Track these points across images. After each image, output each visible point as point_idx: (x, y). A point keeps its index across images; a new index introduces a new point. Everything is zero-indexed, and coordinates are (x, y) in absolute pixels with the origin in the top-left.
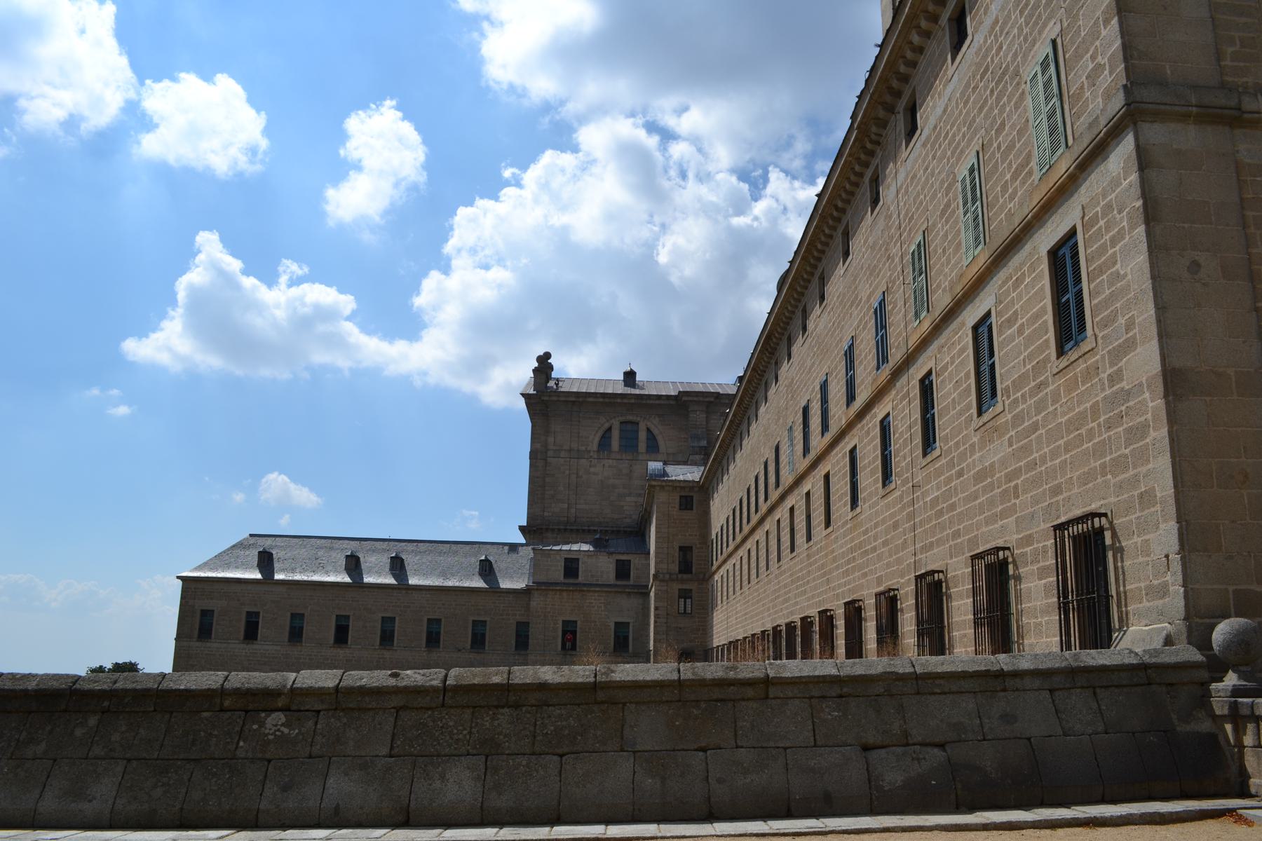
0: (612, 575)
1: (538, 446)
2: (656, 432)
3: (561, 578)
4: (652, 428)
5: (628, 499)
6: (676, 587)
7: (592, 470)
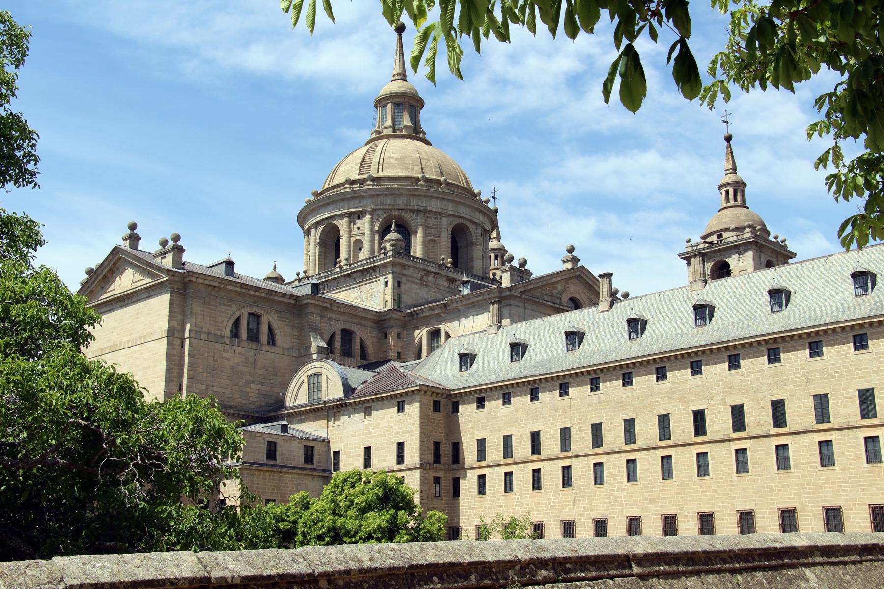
0: (302, 459)
1: (175, 324)
2: (275, 326)
3: (265, 461)
4: (272, 322)
5: (253, 386)
6: (433, 474)
7: (225, 355)
